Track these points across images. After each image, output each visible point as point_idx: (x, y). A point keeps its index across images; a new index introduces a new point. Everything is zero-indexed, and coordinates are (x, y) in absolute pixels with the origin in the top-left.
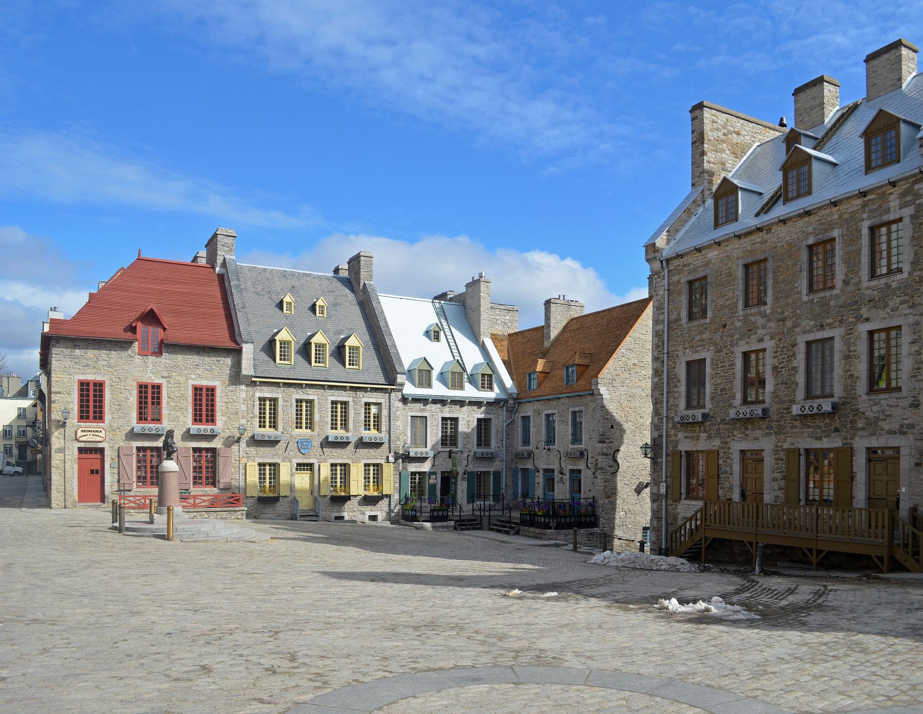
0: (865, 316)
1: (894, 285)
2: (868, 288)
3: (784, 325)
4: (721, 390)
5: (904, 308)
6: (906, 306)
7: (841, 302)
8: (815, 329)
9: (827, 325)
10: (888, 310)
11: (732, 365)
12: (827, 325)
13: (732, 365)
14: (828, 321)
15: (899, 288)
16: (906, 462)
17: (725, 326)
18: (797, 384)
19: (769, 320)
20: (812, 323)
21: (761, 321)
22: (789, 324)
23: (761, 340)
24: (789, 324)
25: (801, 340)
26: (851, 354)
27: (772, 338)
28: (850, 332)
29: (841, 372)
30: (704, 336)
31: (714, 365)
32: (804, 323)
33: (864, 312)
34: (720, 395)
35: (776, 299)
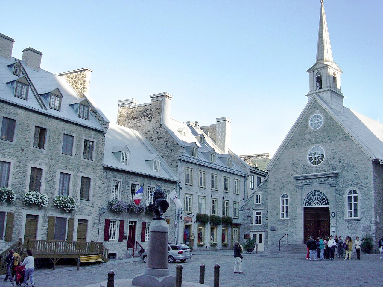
0: (81, 170)
1: (90, 163)
2: (82, 161)
3: (52, 162)
4: (18, 182)
5: (92, 173)
6: (93, 172)
7: (73, 162)
8: (64, 169)
9: (68, 169)
10: (88, 171)
11: (26, 171)
12: (68, 169)
13: (26, 171)
14: (69, 167)
15: (91, 165)
16: (90, 224)
17: (23, 150)
18: (55, 189)
19: (45, 157)
20: (63, 165)
21: (41, 156)
22: (54, 162)
23: (41, 165)
24: (54, 162)
25: (59, 171)
26: (76, 183)
27: (46, 165)
28: (76, 175)
29: (72, 189)
30: (11, 151)
31: (16, 169)
32: (60, 164)
33: (81, 168)
34: (17, 185)
35: (49, 150)
